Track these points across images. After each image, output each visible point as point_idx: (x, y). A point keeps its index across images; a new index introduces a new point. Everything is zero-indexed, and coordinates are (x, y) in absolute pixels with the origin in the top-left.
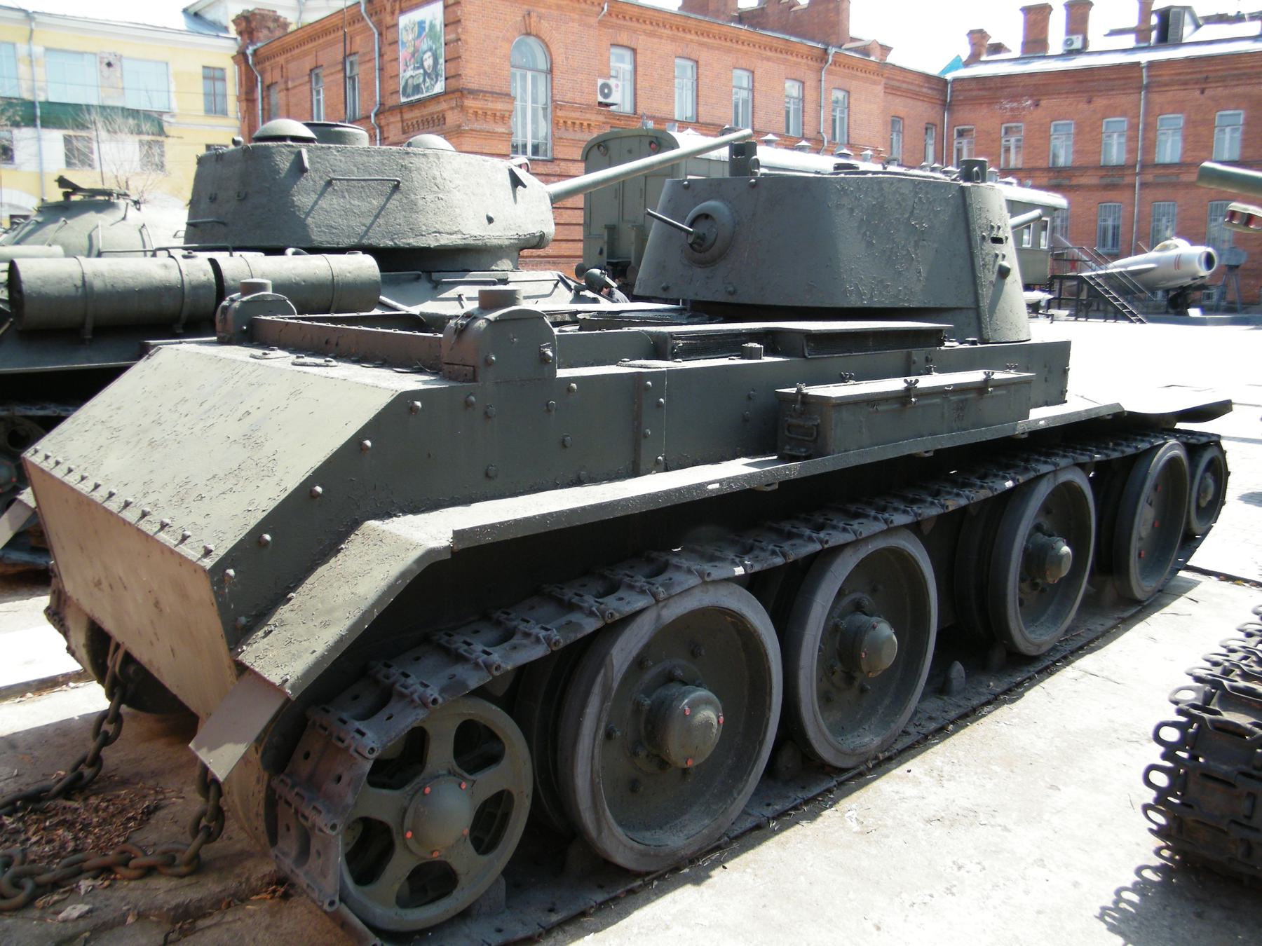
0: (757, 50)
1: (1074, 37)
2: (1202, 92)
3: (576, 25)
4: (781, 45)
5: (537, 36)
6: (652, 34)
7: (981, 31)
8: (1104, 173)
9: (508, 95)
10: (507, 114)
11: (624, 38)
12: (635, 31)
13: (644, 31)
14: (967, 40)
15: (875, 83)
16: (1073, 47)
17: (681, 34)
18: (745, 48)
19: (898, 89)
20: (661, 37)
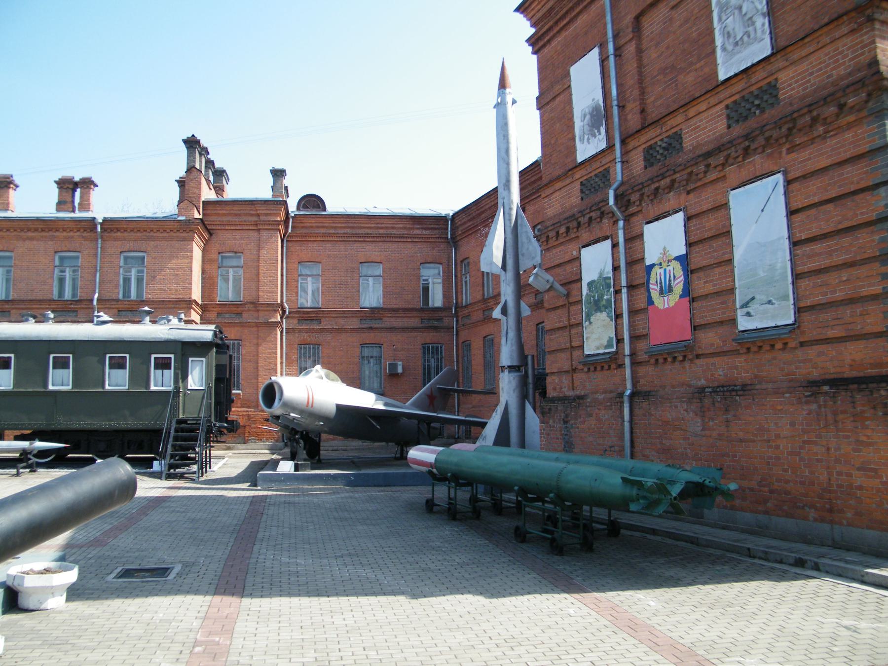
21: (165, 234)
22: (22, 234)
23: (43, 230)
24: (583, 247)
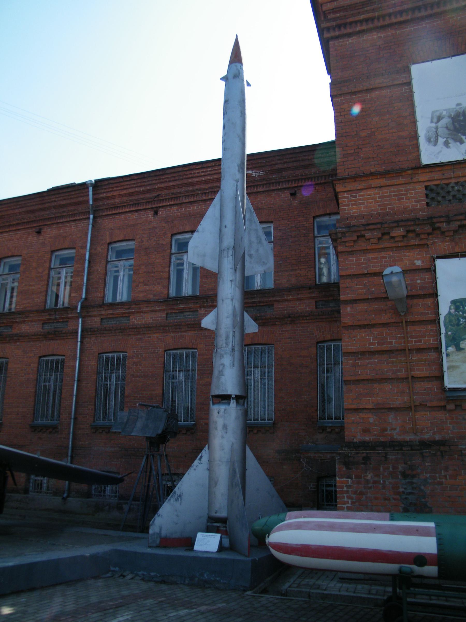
2: (156, 213)
8: (45, 317)
24: (439, 258)
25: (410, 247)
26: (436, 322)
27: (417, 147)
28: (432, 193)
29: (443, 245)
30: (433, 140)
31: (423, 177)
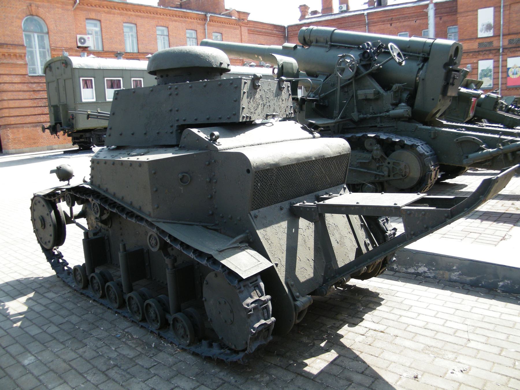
0: (169, 17)
1: (343, 5)
2: (391, 25)
3: (60, 10)
4: (181, 14)
5: (37, 16)
6: (109, 13)
7: (305, 5)
9: (23, 45)
10: (23, 55)
11: (93, 15)
12: (99, 12)
13: (104, 11)
14: (299, 10)
15: (235, 29)
16: (343, 10)
17: (125, 12)
18: (162, 17)
19: (260, 32)
20: (114, 14)
21: (229, 25)
22: (172, 18)
23: (182, 17)
25: (473, 58)
26: (477, 74)
27: (477, 32)
28: (480, 44)
29: (481, 57)
30: (481, 31)
31: (478, 41)
